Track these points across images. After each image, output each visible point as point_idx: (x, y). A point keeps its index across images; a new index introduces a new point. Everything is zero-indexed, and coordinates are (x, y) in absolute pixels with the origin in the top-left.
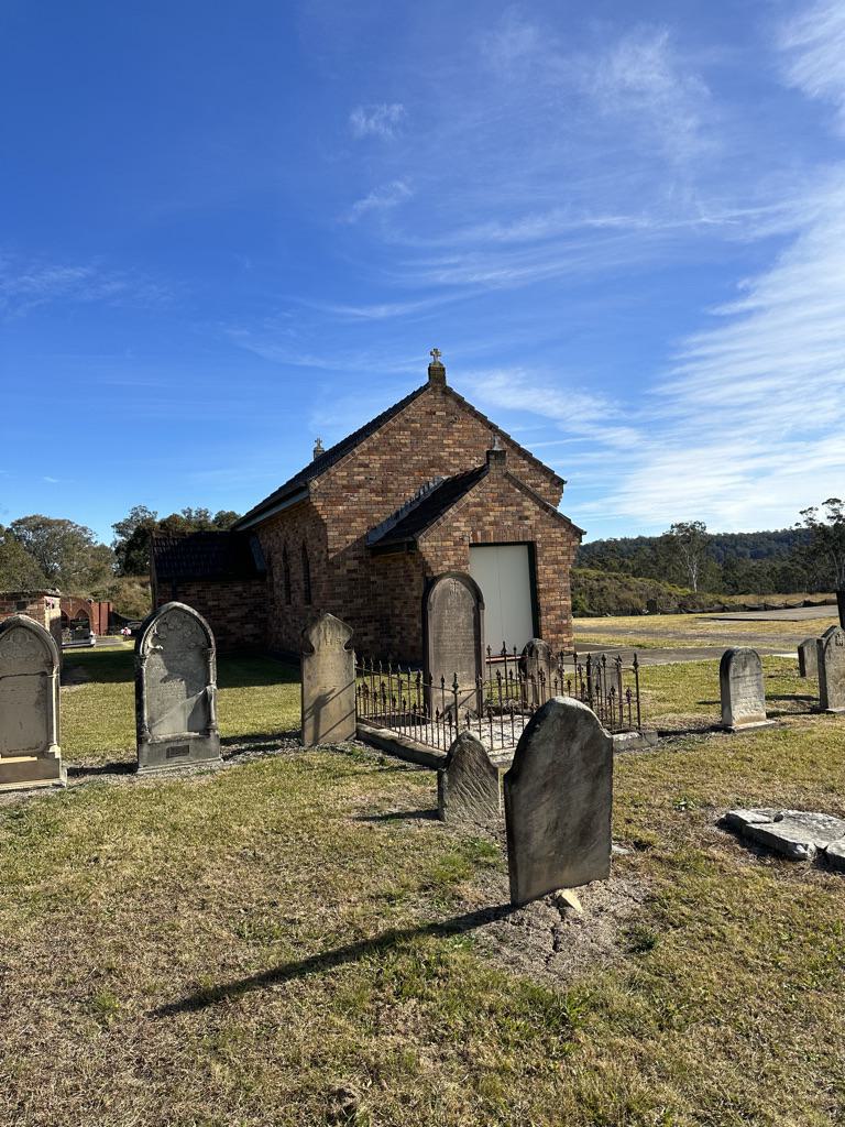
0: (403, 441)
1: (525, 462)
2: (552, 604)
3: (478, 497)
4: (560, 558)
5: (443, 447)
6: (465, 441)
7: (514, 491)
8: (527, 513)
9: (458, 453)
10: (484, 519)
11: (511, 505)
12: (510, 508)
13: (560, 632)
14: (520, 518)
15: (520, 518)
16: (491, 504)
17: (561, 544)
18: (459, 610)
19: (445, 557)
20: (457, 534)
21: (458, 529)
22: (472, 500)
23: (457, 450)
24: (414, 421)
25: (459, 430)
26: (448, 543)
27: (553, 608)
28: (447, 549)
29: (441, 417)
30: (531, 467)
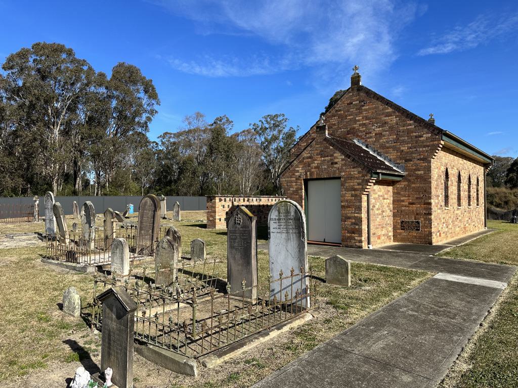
0: (333, 123)
1: (412, 122)
2: (349, 215)
3: (309, 153)
4: (357, 187)
5: (355, 121)
6: (370, 115)
7: (329, 148)
8: (336, 160)
9: (365, 124)
10: (312, 165)
11: (327, 156)
12: (326, 158)
13: (354, 233)
14: (332, 164)
15: (332, 164)
16: (315, 157)
17: (357, 178)
18: (149, 211)
19: (291, 186)
20: (297, 174)
21: (298, 171)
22: (306, 155)
23: (364, 122)
24: (340, 111)
25: (366, 110)
26: (293, 179)
27: (349, 218)
28: (292, 182)
29: (356, 105)
30: (416, 124)
